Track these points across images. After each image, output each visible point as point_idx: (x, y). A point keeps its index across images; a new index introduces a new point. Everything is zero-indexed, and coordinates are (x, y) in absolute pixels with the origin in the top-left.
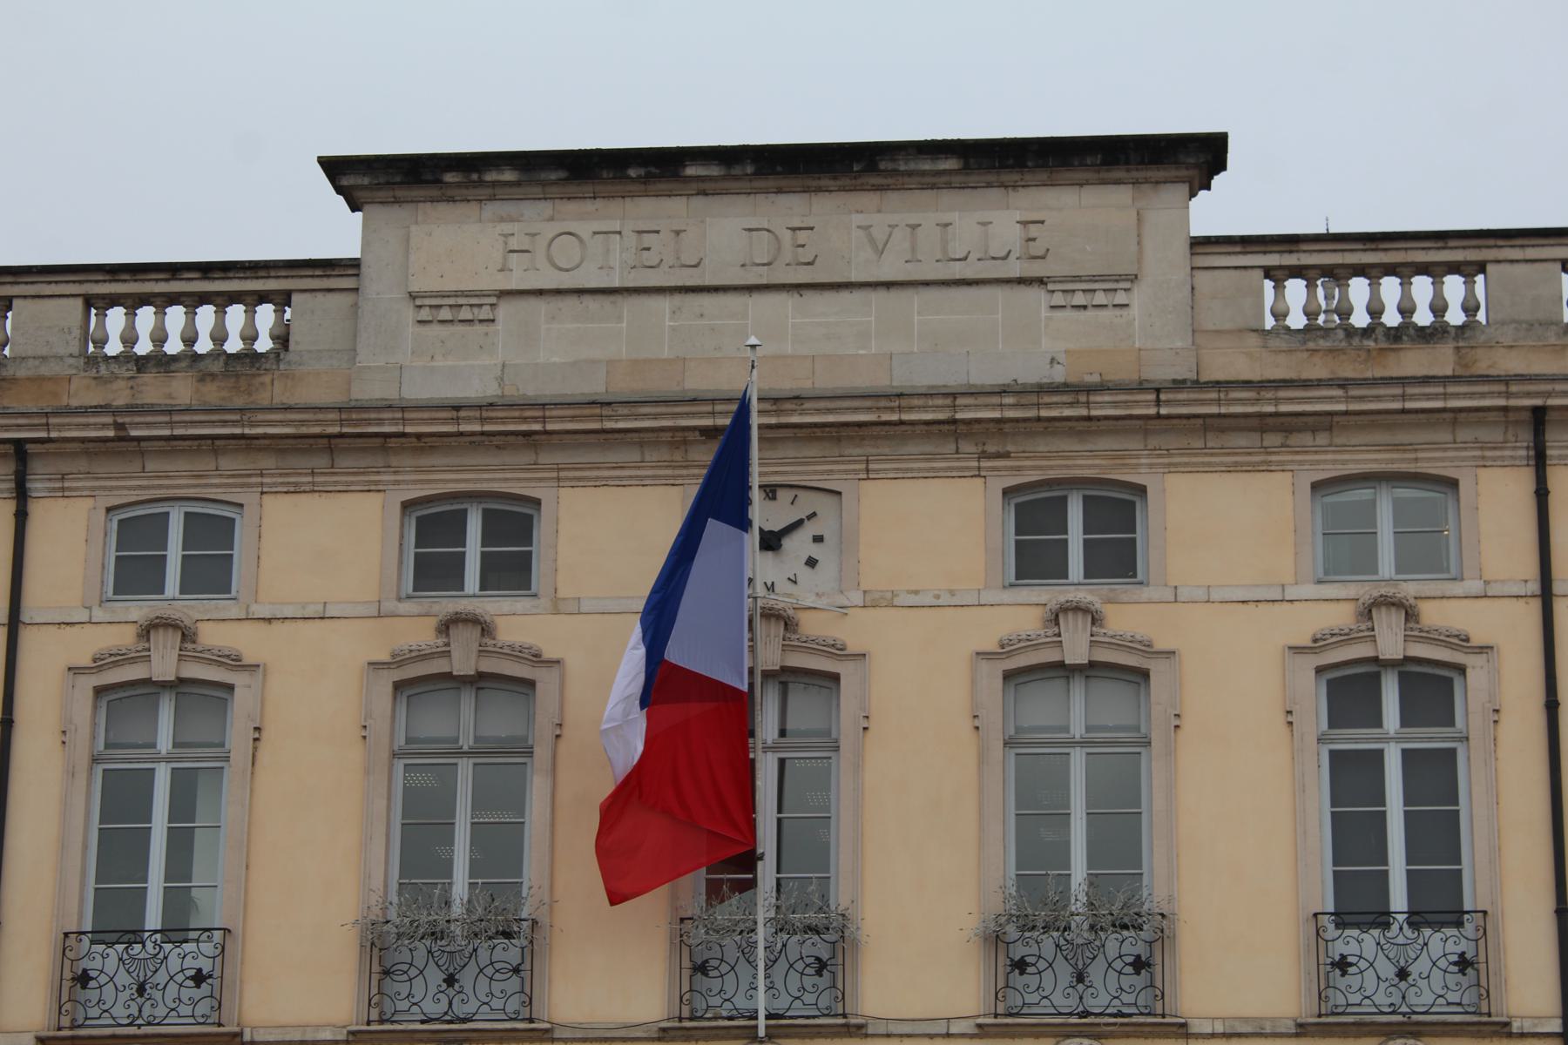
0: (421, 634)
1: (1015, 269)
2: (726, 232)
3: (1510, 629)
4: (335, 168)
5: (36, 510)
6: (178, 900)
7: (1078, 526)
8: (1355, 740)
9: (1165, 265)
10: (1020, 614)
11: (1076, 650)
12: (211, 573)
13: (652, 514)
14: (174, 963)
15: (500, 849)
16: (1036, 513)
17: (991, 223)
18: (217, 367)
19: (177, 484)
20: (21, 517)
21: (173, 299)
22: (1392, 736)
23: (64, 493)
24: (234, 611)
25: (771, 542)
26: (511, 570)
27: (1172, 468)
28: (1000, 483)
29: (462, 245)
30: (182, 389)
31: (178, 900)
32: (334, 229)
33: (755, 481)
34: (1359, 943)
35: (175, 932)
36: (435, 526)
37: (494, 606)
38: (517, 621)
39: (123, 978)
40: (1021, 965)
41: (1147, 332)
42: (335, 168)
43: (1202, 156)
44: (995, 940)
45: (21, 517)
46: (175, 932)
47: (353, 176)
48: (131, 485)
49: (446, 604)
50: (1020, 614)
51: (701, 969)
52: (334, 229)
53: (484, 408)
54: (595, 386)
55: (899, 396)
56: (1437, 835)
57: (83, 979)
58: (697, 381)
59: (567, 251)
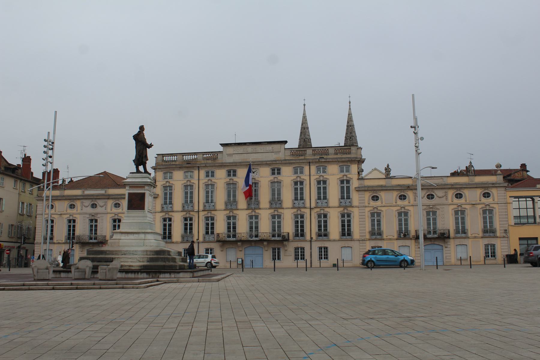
0: (228, 180)
2: (250, 149)
3: (307, 178)
6: (212, 200)
7: (276, 171)
8: (296, 187)
9: (283, 150)
10: (272, 178)
11: (276, 181)
12: (213, 176)
13: (245, 171)
15: (234, 196)
16: (273, 170)
17: (269, 148)
19: (210, 169)
22: (299, 186)
25: (253, 173)
26: (235, 175)
29: (230, 150)
31: (212, 200)
32: (221, 149)
34: (296, 202)
35: (212, 202)
36: (229, 172)
37: (234, 178)
38: (235, 179)
41: (281, 156)
43: (286, 142)
44: (270, 202)
46: (212, 202)
47: (222, 145)
48: (207, 169)
49: (230, 178)
50: (272, 178)
52: (221, 149)
53: (232, 163)
54: (240, 161)
55: (262, 162)
56: (302, 194)
58: (248, 160)
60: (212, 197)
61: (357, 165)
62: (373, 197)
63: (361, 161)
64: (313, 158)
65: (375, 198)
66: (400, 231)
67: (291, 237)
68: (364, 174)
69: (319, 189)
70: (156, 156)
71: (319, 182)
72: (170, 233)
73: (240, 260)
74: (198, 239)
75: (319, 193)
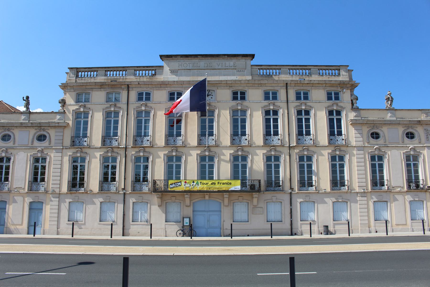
1: (233, 68)
2: (202, 63)
4: (161, 57)
5: (130, 92)
9: (249, 68)
14: (145, 139)
17: (231, 62)
18: (148, 77)
20: (128, 92)
21: (144, 70)
23: (132, 90)
24: (151, 102)
27: (249, 89)
28: (231, 90)
30: (145, 79)
31: (145, 133)
33: (207, 89)
35: (145, 136)
39: (140, 140)
40: (234, 140)
42: (161, 57)
43: (253, 56)
45: (128, 92)
51: (201, 140)
57: (136, 140)
59: (185, 65)
60: (145, 129)
61: (349, 91)
62: (372, 134)
63: (352, 86)
64: (290, 79)
65: (375, 136)
66: (409, 181)
67: (263, 188)
68: (359, 104)
69: (299, 121)
70: (68, 71)
71: (299, 113)
72: (82, 179)
73: (187, 221)
74: (124, 189)
75: (300, 127)
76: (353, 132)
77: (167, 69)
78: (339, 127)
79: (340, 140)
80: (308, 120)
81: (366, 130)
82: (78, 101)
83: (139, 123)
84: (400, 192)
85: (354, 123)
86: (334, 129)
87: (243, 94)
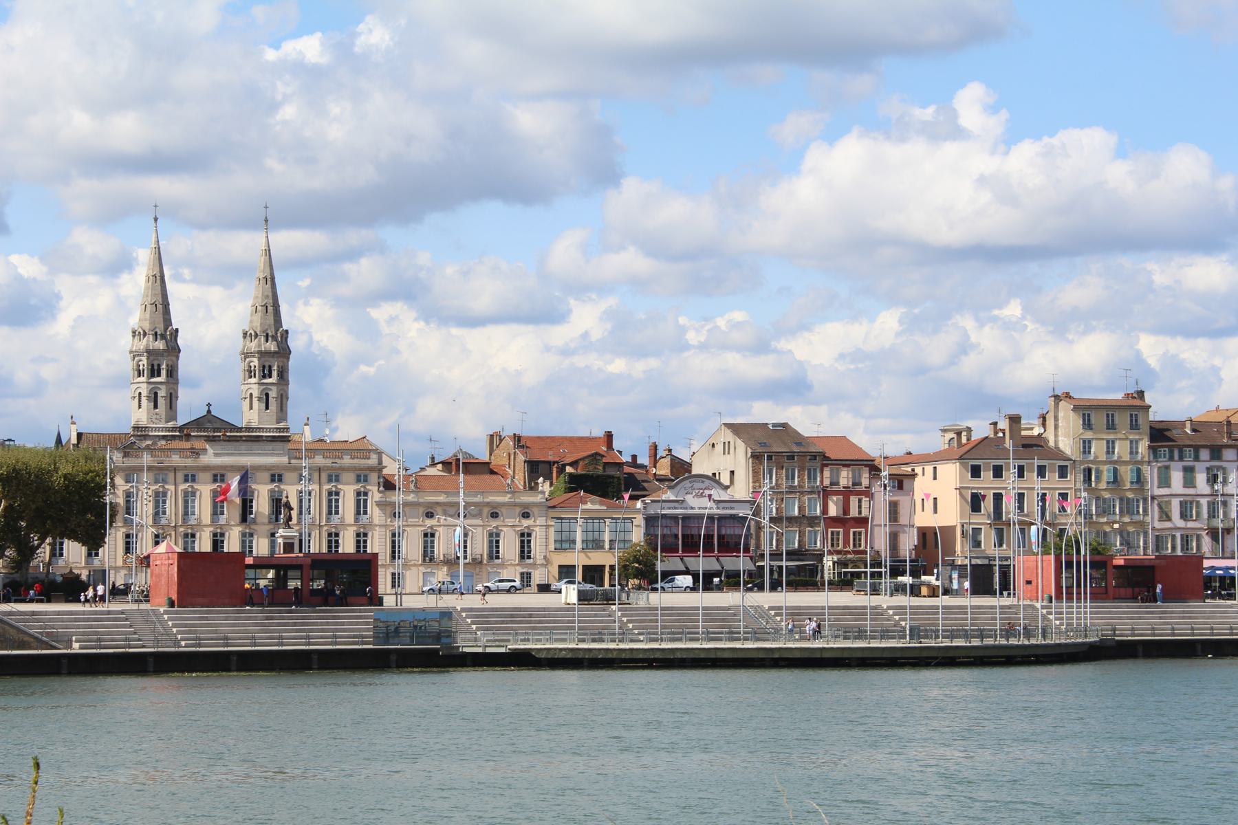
16: (273, 476)
69: (330, 501)
75: (330, 507)
76: (377, 511)
77: (211, 451)
78: (365, 507)
79: (364, 519)
80: (337, 501)
81: (389, 510)
82: (127, 482)
83: (186, 502)
84: (415, 565)
85: (379, 504)
86: (361, 508)
87: (280, 476)
